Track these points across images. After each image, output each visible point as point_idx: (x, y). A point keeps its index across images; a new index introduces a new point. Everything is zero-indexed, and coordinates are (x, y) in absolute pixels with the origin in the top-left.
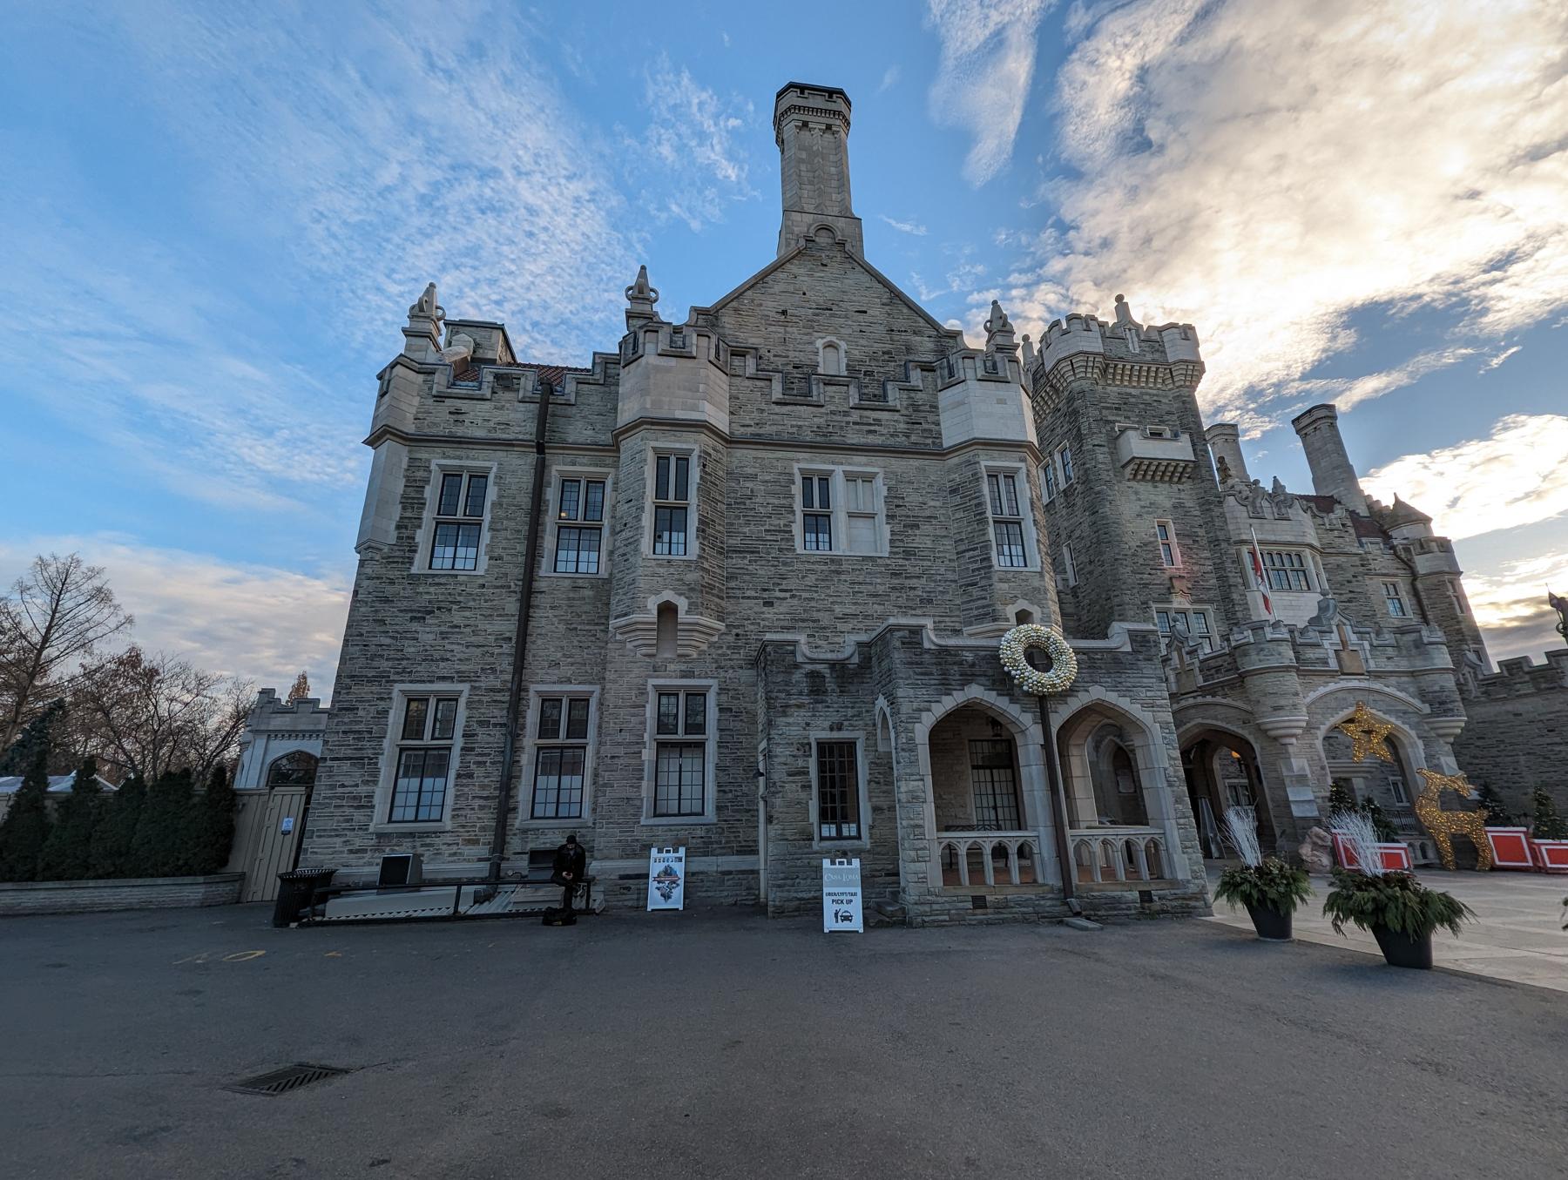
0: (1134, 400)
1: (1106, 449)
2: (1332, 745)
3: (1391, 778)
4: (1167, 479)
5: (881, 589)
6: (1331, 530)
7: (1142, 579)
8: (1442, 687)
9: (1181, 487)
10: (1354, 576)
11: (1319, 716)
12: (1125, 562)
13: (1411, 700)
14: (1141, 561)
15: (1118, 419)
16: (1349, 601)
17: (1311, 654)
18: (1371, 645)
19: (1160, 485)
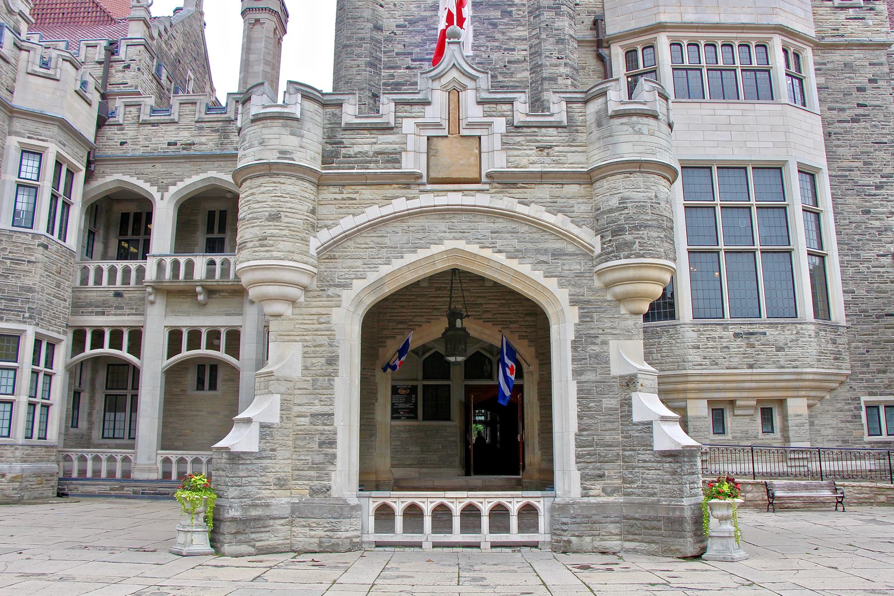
2: (752, 346)
3: (864, 399)
7: (393, 76)
8: (623, 200)
11: (359, 263)
12: (357, 51)
13: (574, 229)
14: (399, 48)
18: (510, 124)
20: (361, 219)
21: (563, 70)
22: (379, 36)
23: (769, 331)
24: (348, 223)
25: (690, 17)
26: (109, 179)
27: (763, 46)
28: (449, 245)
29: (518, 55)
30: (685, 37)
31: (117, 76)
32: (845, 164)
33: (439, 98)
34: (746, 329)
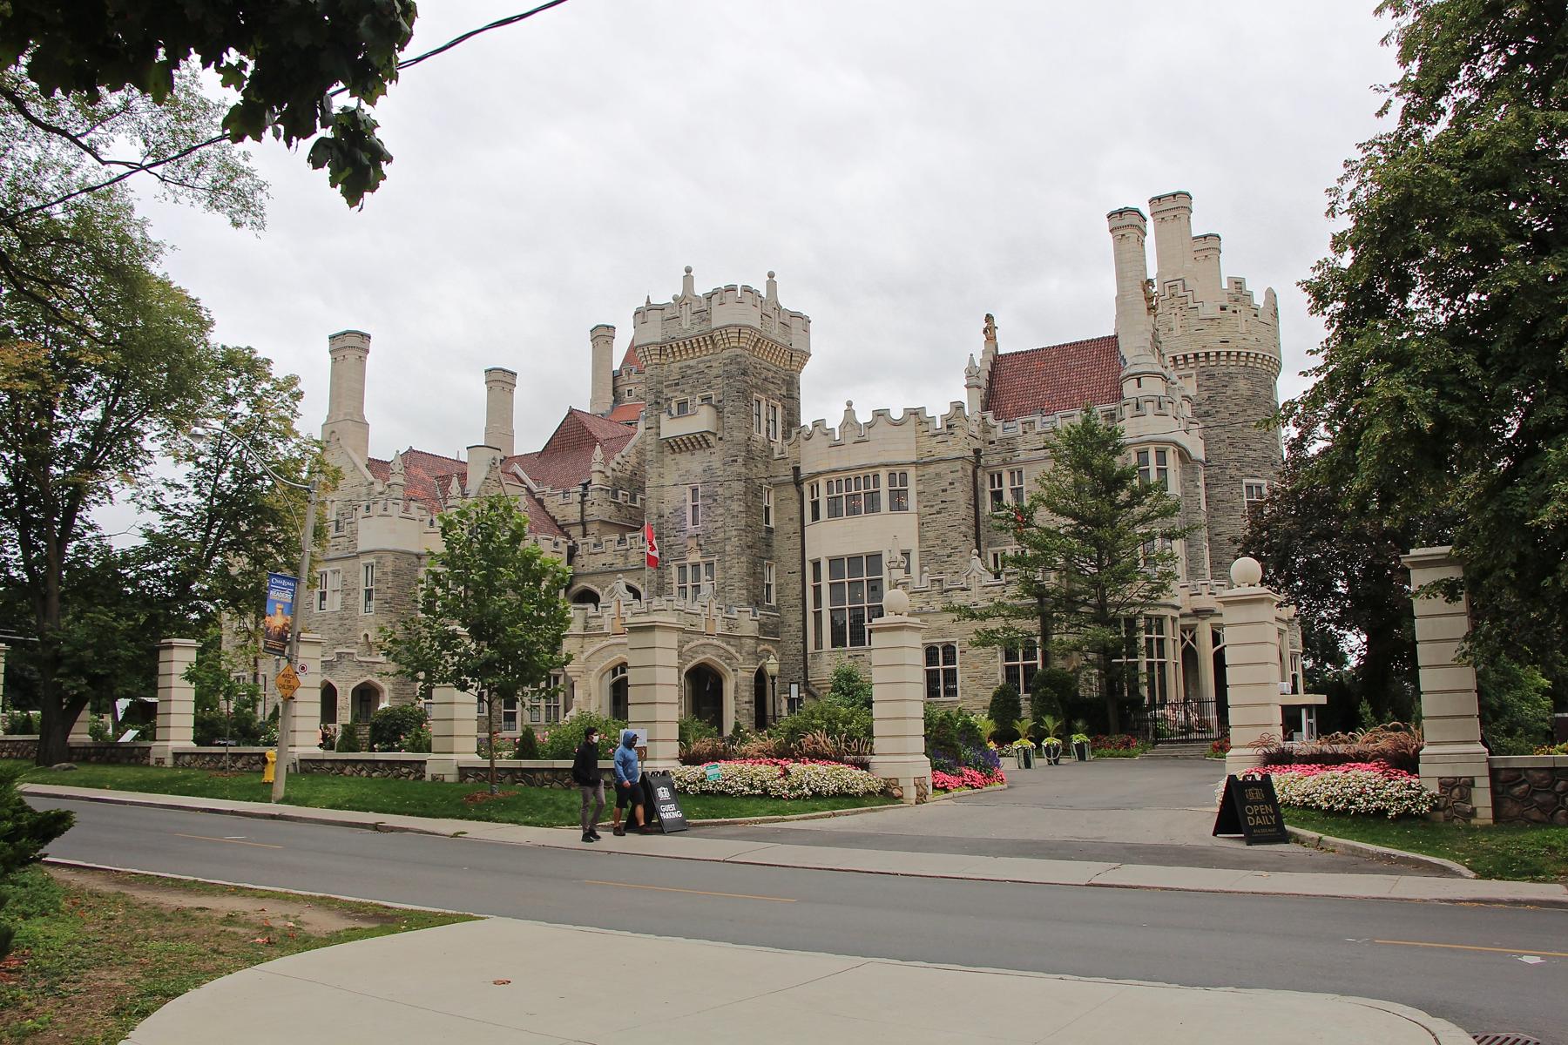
0: (689, 372)
1: (654, 431)
2: (857, 662)
4: (698, 447)
5: (336, 626)
6: (935, 436)
9: (712, 450)
10: (950, 484)
15: (675, 394)
16: (938, 513)
17: (593, 623)
19: (697, 452)
20: (595, 649)
21: (734, 533)
22: (660, 521)
23: (866, 654)
24: (591, 650)
25: (833, 466)
26: (579, 585)
27: (876, 476)
28: (619, 655)
29: (719, 524)
30: (834, 477)
31: (589, 511)
32: (931, 543)
33: (614, 604)
34: (855, 653)
